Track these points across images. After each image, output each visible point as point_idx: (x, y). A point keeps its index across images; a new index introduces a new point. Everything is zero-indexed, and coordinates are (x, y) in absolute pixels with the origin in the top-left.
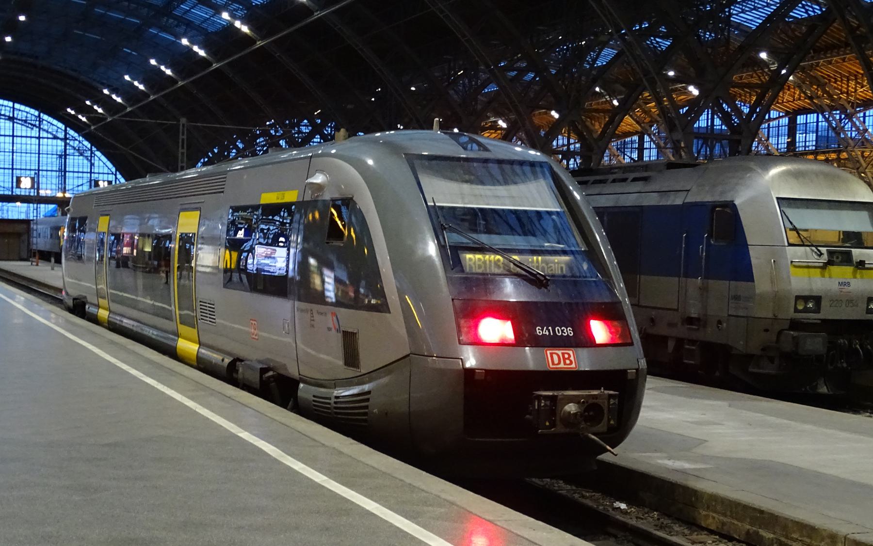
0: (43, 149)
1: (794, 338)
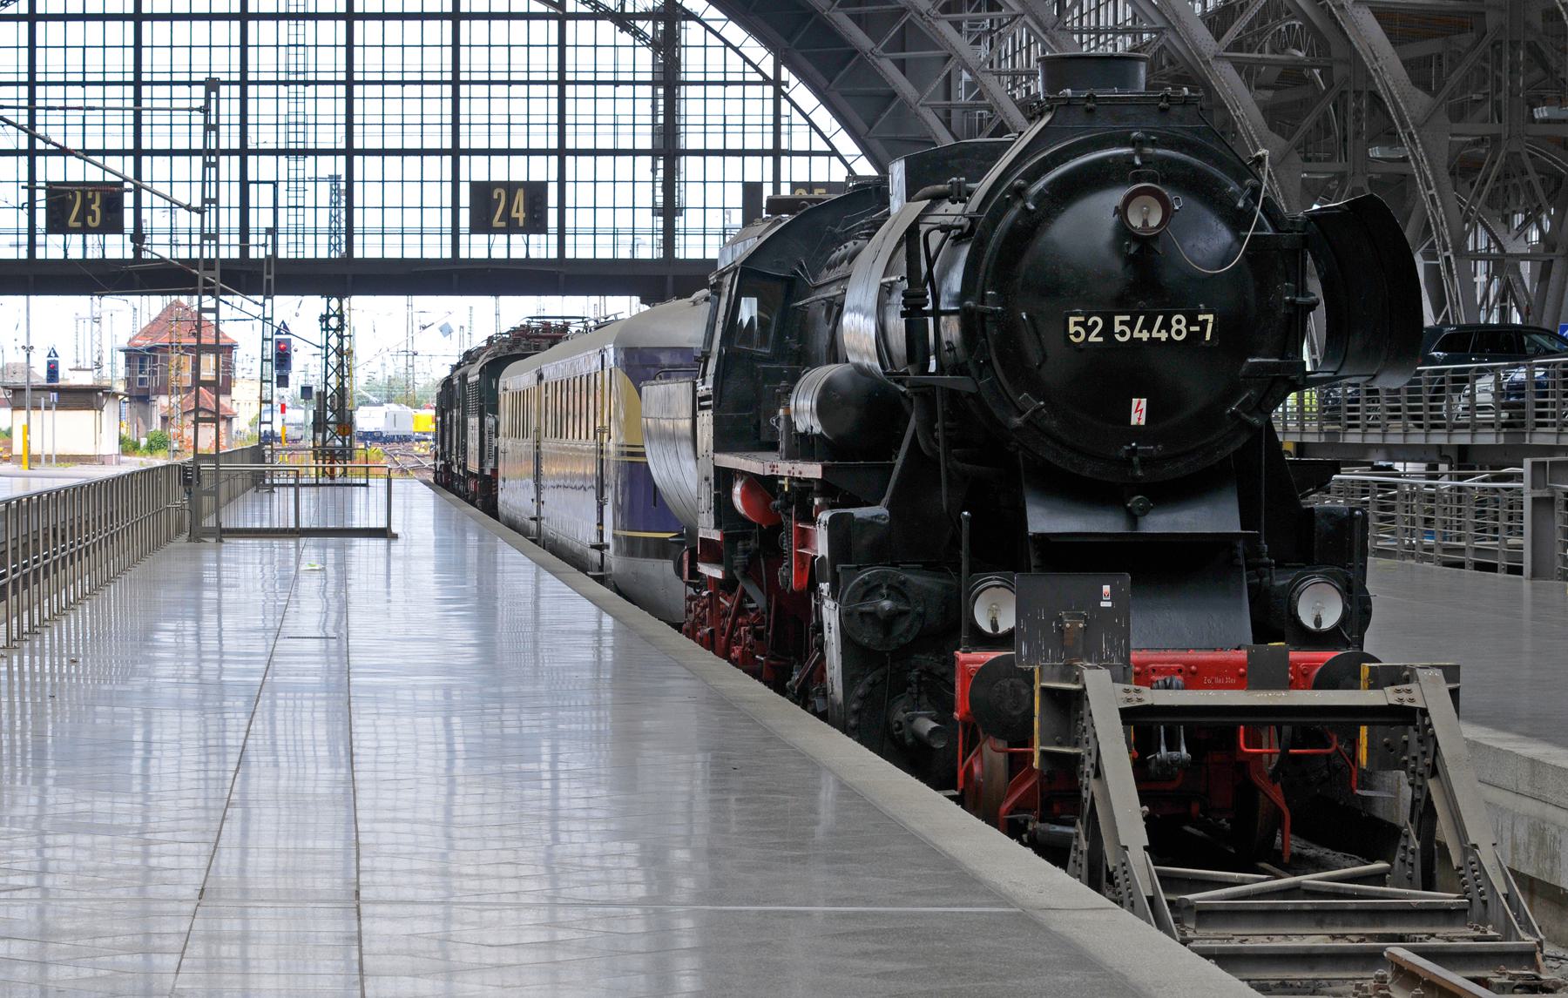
0: (580, 62)
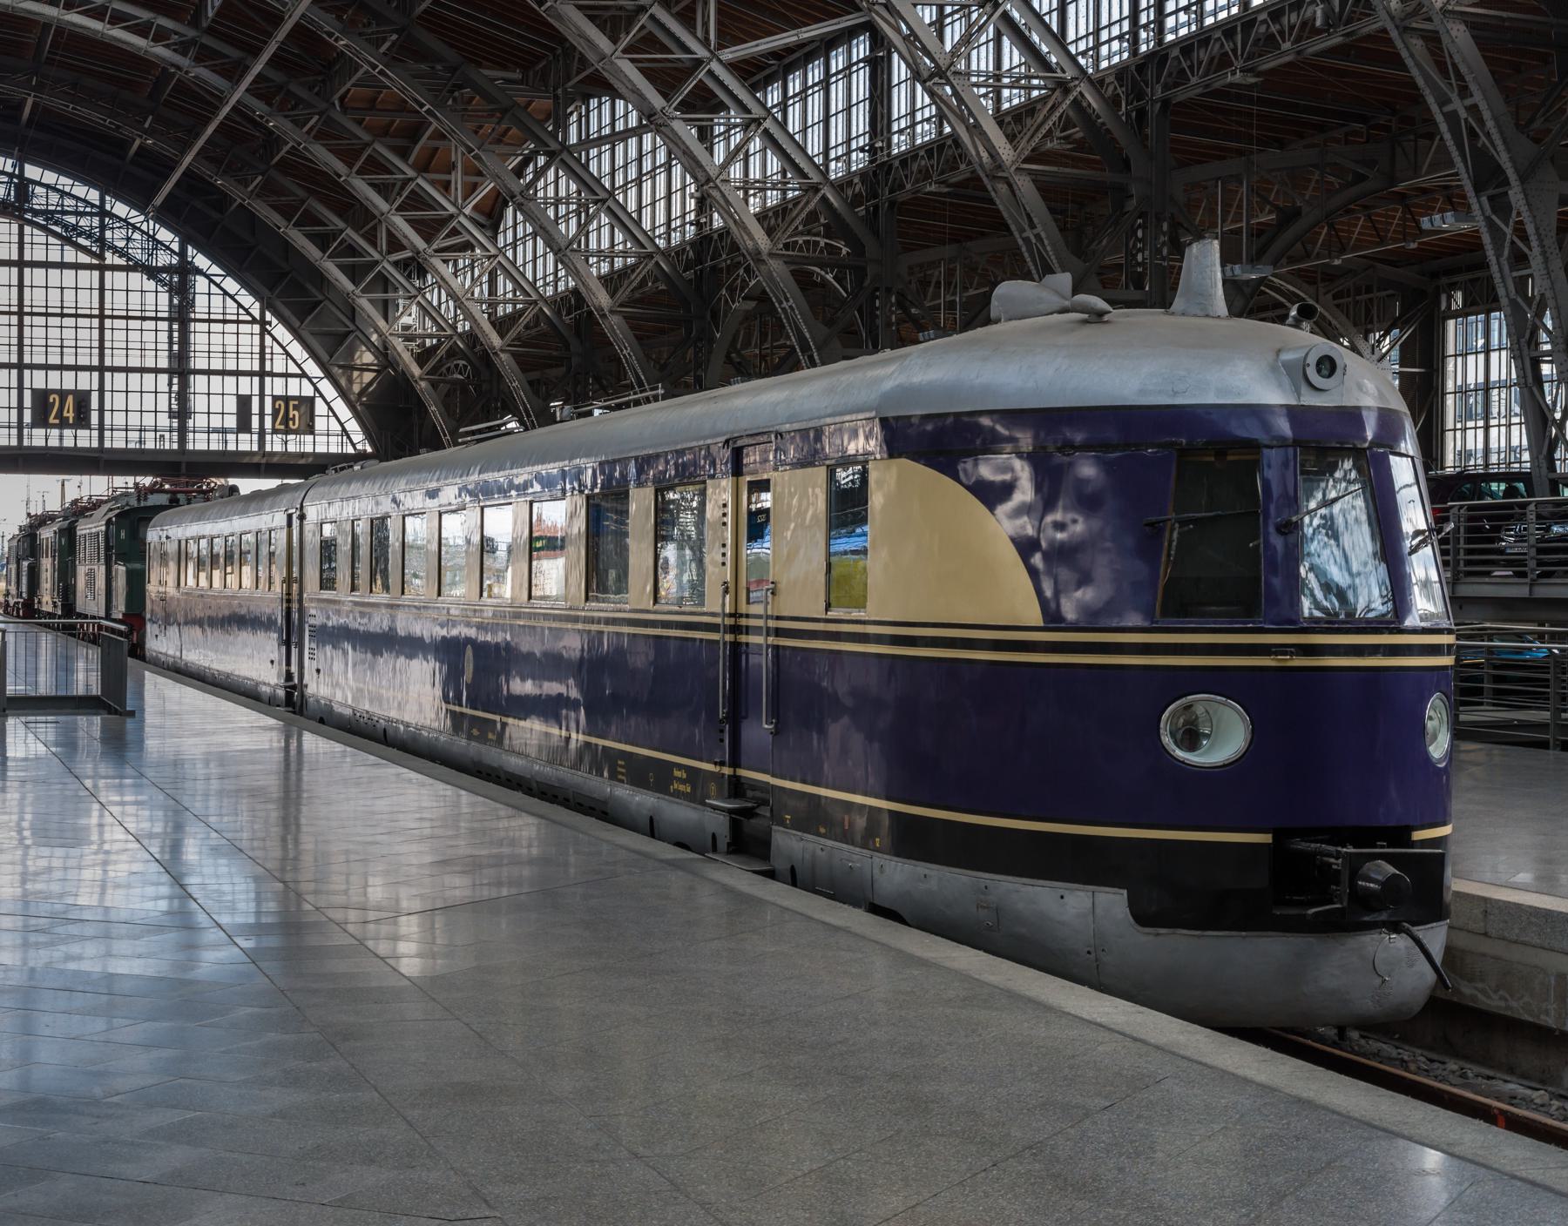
0: (116, 302)
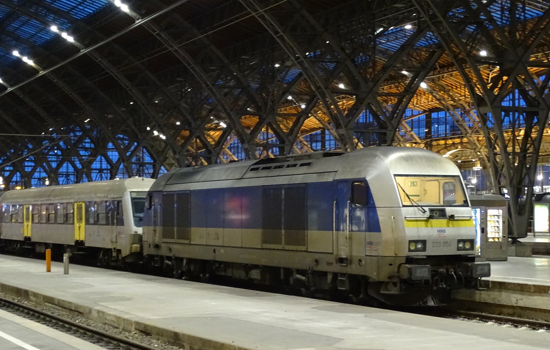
1: (409, 269)
